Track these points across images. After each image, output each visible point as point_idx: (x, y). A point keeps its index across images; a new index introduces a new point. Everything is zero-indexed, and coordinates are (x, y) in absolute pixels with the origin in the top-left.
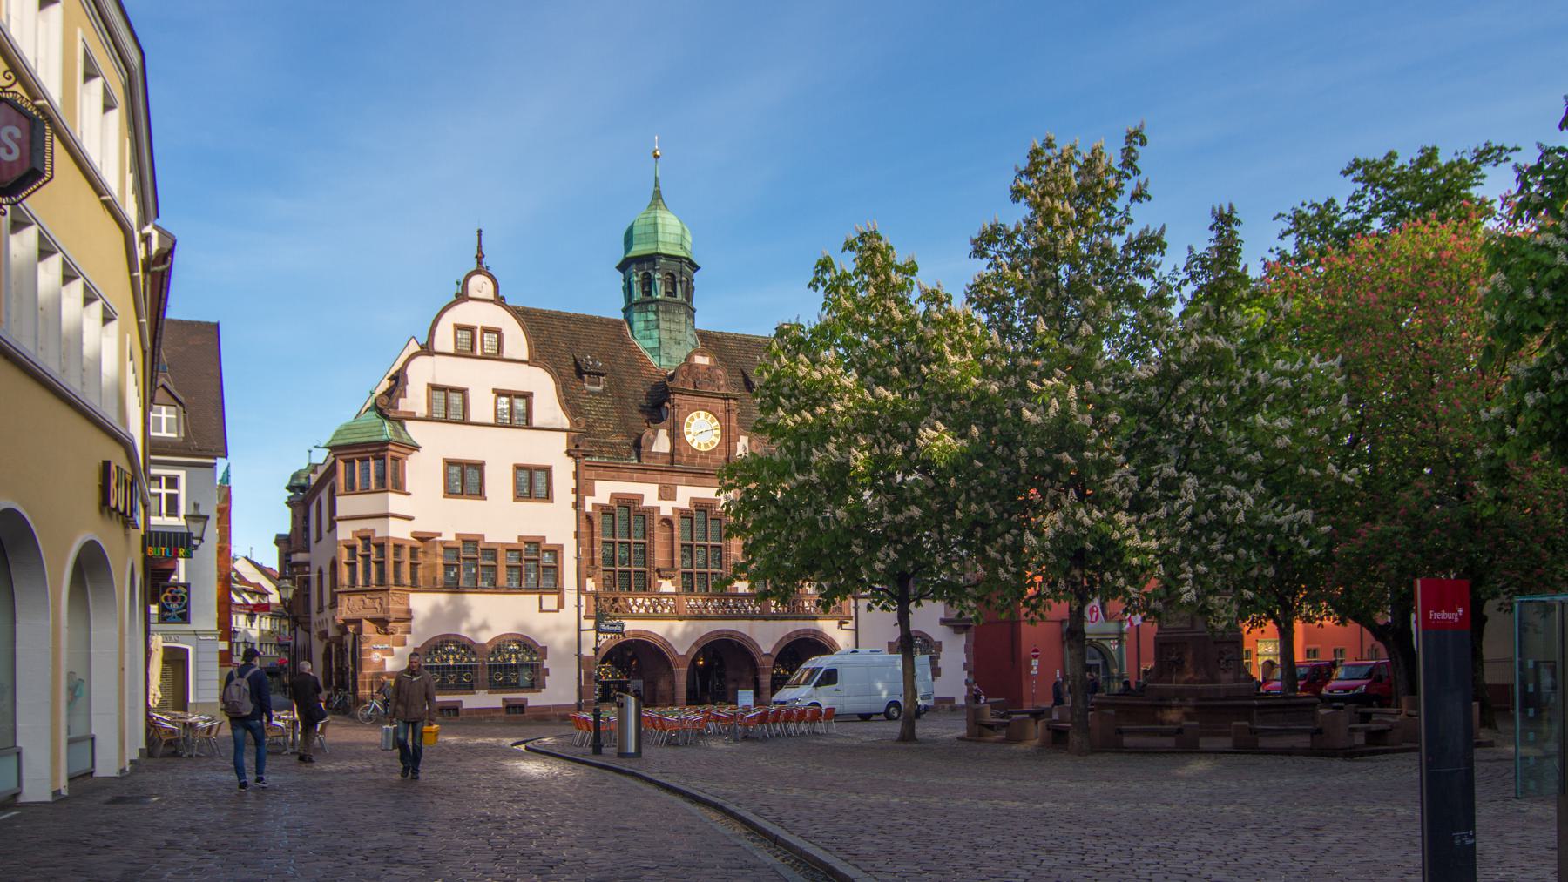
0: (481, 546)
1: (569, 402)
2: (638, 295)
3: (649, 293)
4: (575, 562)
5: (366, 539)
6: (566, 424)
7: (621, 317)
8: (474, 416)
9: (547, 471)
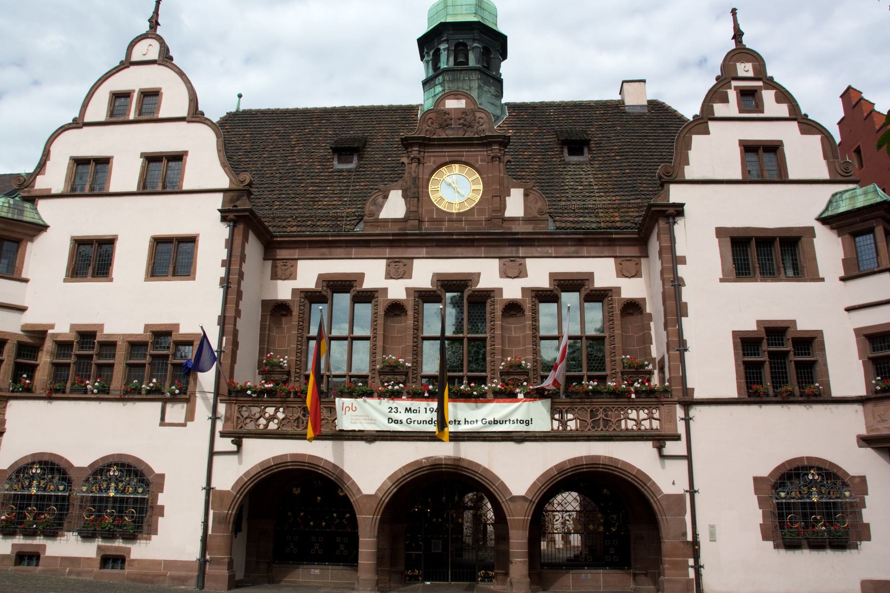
0: (99, 338)
2: (431, 73)
6: (223, 181)
9: (192, 240)
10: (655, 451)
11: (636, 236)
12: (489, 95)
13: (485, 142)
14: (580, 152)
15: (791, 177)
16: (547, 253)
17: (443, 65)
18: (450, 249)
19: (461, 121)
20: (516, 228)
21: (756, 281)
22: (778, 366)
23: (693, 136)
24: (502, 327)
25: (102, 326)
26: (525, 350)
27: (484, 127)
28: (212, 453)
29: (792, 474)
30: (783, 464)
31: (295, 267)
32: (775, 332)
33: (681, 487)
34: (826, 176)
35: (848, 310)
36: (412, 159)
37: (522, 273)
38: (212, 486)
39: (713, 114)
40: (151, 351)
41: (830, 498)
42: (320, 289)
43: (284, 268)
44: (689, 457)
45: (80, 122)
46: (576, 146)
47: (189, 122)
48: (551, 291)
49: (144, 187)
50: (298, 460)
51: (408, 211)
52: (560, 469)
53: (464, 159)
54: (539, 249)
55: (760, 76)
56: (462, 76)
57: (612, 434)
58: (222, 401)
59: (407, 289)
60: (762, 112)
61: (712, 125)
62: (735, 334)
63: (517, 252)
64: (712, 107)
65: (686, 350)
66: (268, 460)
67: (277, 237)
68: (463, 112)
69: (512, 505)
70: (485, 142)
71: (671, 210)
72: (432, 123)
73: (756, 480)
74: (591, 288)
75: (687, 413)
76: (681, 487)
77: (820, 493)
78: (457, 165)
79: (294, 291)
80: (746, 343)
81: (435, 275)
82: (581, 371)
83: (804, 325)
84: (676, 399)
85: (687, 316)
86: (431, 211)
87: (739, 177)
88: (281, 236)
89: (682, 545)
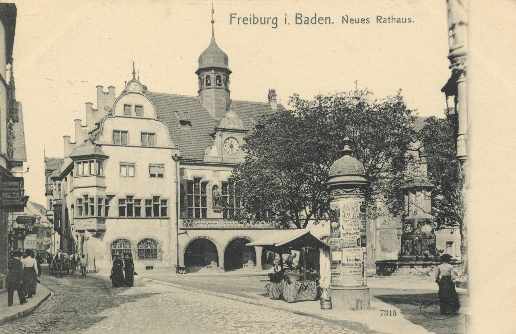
1: (172, 135)
3: (210, 85)
5: (86, 196)
7: (197, 94)
8: (132, 142)
28: (178, 234)
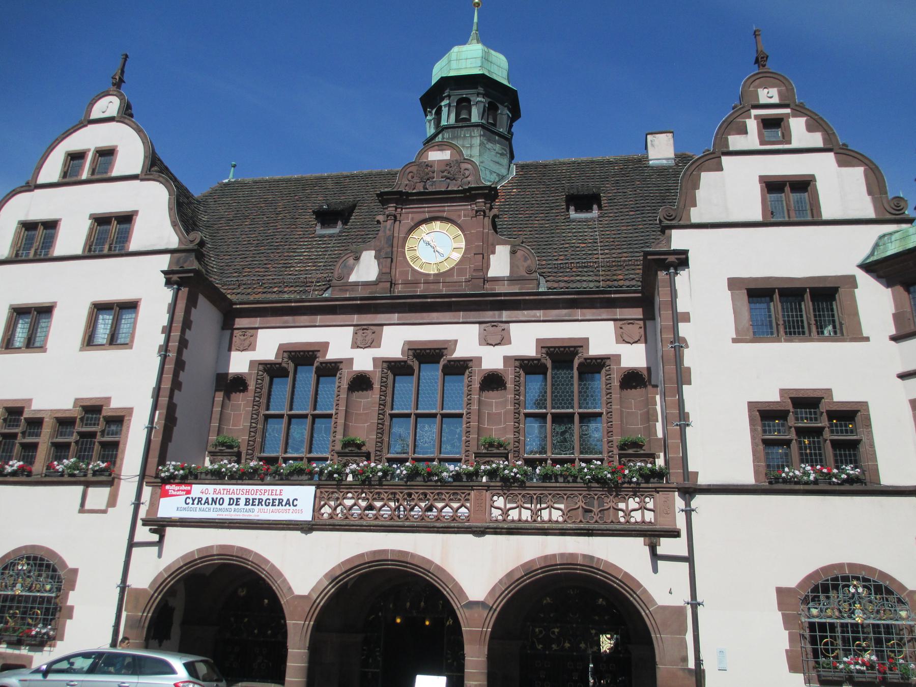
0: (26, 414)
4: (144, 434)
6: (172, 240)
10: (647, 549)
11: (640, 295)
12: (493, 153)
13: (468, 195)
14: (589, 209)
15: (826, 216)
16: (534, 316)
17: (444, 122)
18: (425, 315)
19: (445, 174)
20: (499, 289)
21: (780, 341)
22: (814, 445)
23: (703, 174)
24: (480, 401)
25: (30, 401)
26: (504, 428)
27: (469, 179)
28: (131, 545)
29: (827, 584)
30: (816, 573)
31: (254, 336)
32: (806, 402)
33: (681, 598)
34: (871, 214)
35: (903, 376)
36: (388, 216)
37: (504, 340)
38: (128, 583)
39: (727, 146)
40: (79, 428)
41: (880, 619)
42: (280, 360)
43: (242, 338)
44: (689, 559)
45: (32, 184)
46: (583, 201)
47: (142, 180)
48: (539, 360)
49: (90, 250)
50: (226, 552)
51: (381, 274)
52: (528, 569)
53: (445, 215)
54: (525, 312)
55: (787, 102)
56: (462, 132)
57: (591, 526)
58: (148, 484)
59: (375, 359)
60: (790, 143)
61: (724, 159)
62: (751, 405)
63: (500, 316)
64: (727, 140)
65: (688, 425)
66: (192, 553)
67: (236, 304)
68: (448, 164)
69: (468, 612)
70: (468, 195)
71: (671, 258)
72: (413, 177)
73: (780, 591)
74: (585, 356)
75: (688, 504)
76: (681, 598)
77: (864, 611)
78: (438, 223)
79: (252, 363)
80: (765, 416)
81: (407, 343)
82: (573, 453)
83: (842, 395)
84: (675, 485)
85: (689, 383)
86: (407, 273)
87: (759, 217)
88: (241, 304)
89: (681, 673)
